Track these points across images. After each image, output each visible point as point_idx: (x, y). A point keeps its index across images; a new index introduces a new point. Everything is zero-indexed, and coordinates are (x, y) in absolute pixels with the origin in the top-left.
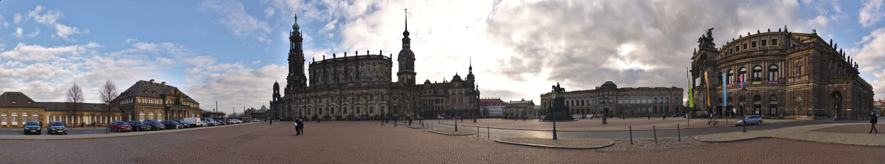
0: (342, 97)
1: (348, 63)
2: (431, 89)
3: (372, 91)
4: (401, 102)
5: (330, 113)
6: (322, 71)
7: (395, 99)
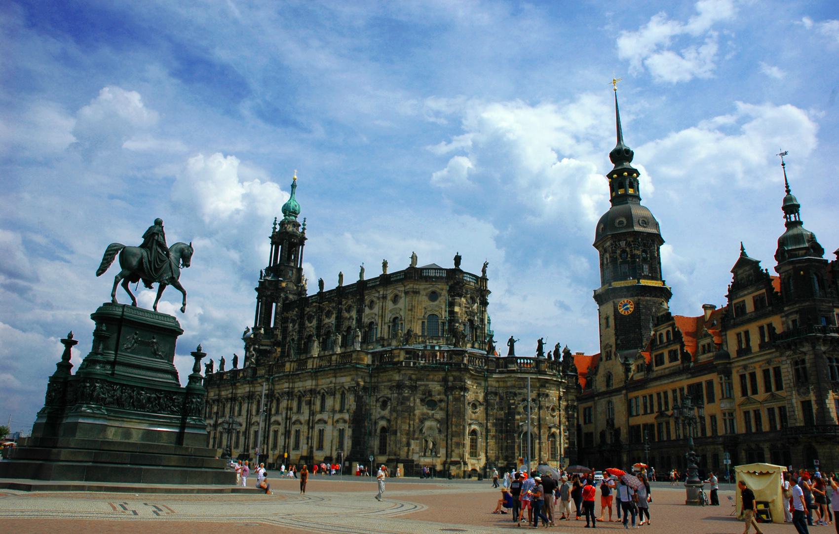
0: (272, 402)
1: (344, 303)
2: (674, 342)
3: (324, 383)
4: (395, 415)
5: (251, 446)
6: (297, 326)
7: (384, 405)
